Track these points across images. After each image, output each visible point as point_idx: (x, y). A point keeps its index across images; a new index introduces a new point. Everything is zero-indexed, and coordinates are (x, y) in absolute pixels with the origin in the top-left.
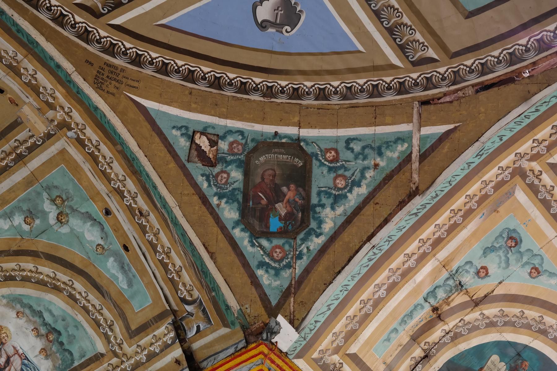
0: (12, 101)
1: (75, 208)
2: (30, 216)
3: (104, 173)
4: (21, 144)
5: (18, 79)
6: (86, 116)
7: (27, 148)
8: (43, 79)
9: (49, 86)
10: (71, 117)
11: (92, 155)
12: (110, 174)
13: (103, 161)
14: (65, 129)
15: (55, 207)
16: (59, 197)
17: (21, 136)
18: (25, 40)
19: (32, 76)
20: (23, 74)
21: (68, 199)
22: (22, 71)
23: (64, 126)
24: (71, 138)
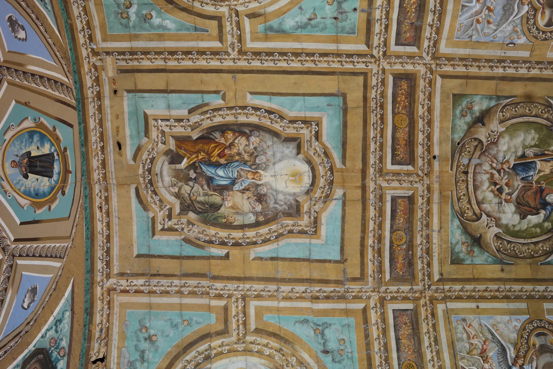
0: (114, 84)
1: (116, 5)
2: (147, 18)
3: (86, 14)
4: (126, 60)
5: (101, 91)
6: (79, 50)
7: (125, 55)
8: (88, 81)
9: (88, 77)
10: (88, 55)
11: (89, 28)
12: (82, 11)
13: (83, 20)
14: (96, 51)
15: (129, 14)
16: (122, 18)
17: (124, 63)
18: (81, 105)
19: (92, 87)
20: (96, 91)
21: (118, 13)
22: (95, 93)
23: (95, 53)
24: (94, 44)
